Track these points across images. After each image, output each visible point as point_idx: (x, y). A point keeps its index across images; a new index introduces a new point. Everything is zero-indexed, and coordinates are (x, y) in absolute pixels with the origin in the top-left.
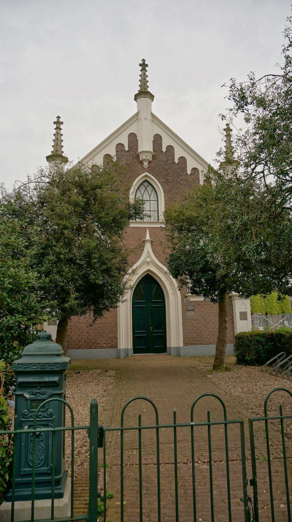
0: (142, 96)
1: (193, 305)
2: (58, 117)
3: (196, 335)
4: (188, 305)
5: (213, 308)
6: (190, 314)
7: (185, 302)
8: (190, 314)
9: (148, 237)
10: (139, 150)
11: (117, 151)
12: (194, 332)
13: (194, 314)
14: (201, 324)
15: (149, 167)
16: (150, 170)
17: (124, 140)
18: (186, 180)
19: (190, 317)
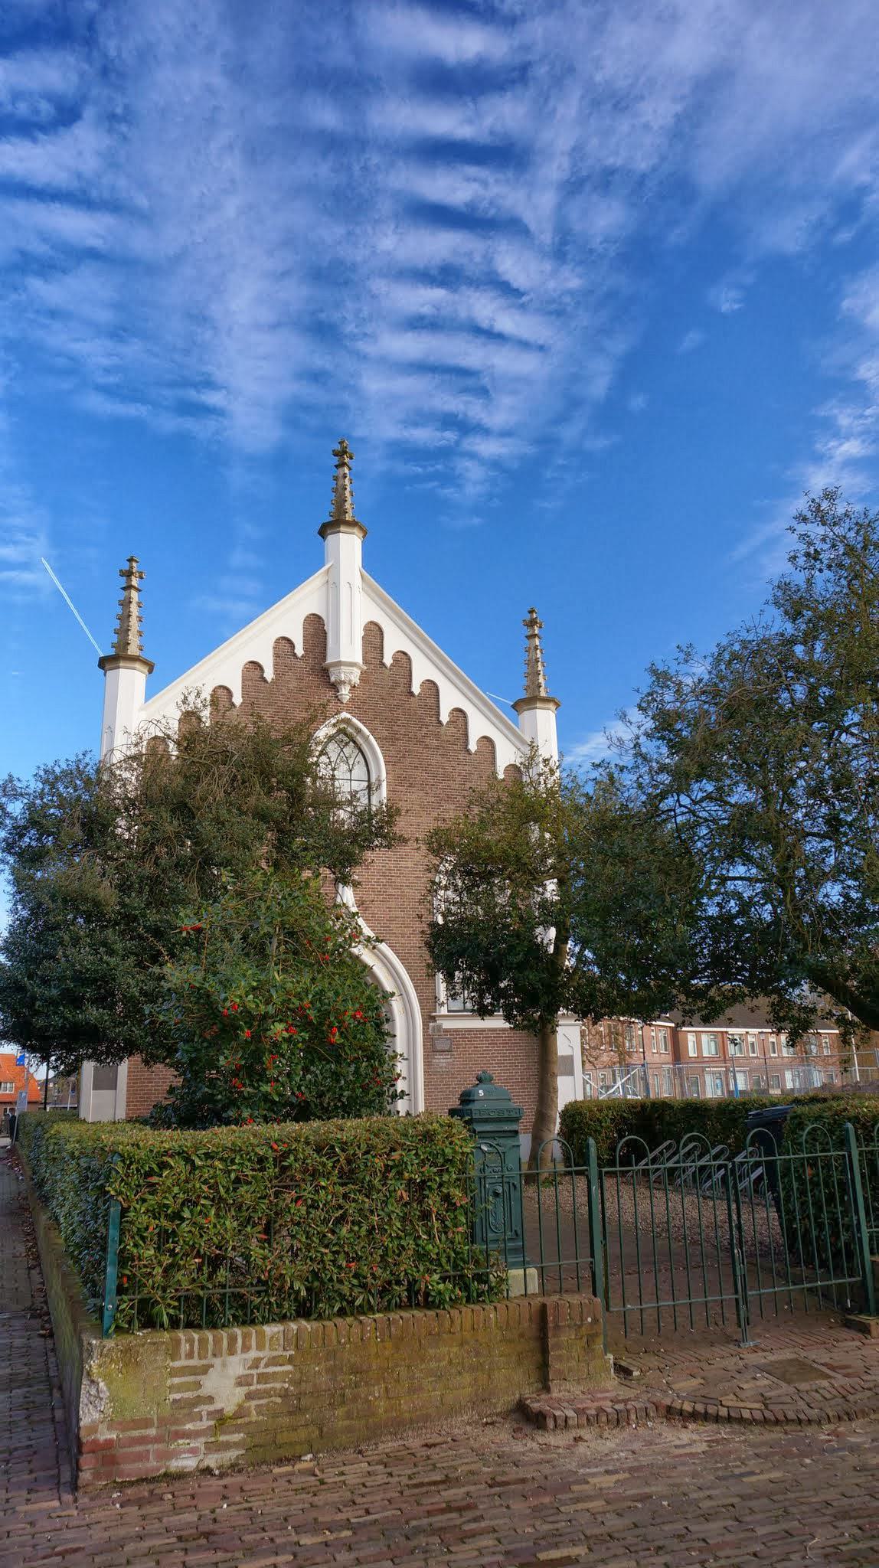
0: (342, 528)
1: (448, 1039)
4: (437, 1039)
7: (430, 1032)
8: (441, 1060)
10: (330, 660)
11: (277, 656)
15: (352, 700)
16: (355, 707)
18: (437, 736)
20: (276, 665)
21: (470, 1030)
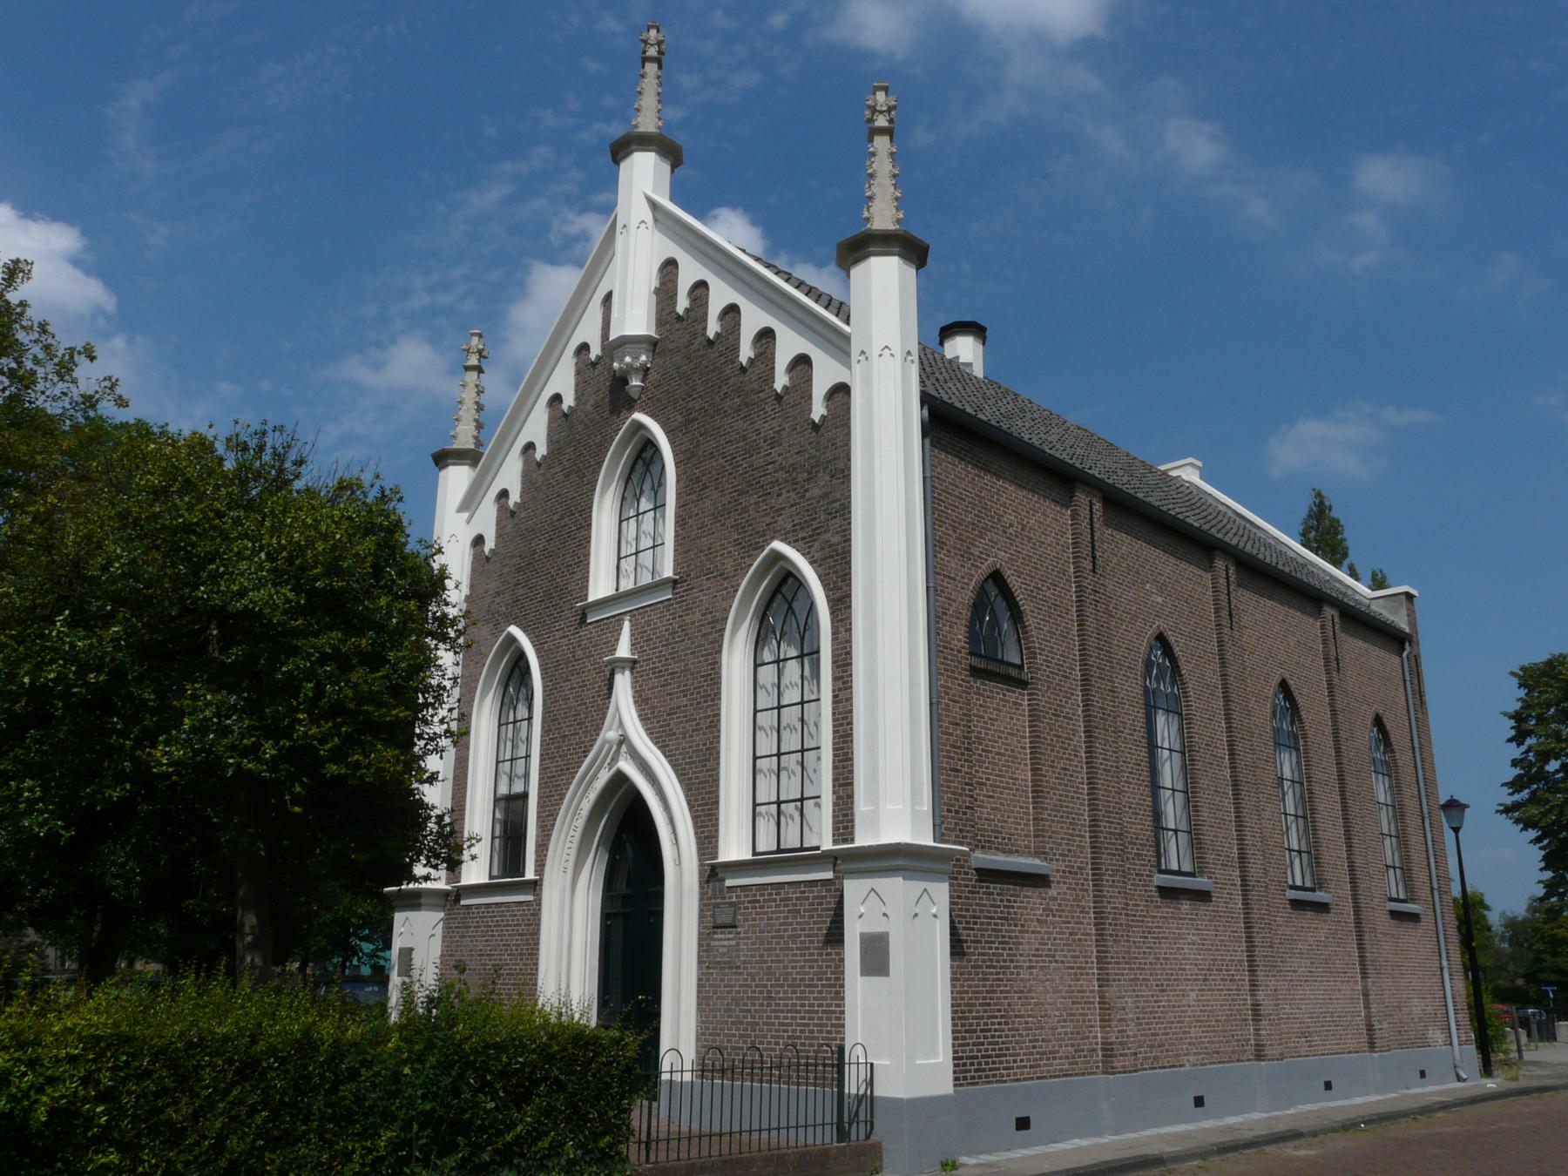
1: (732, 904)
3: (741, 1036)
5: (795, 918)
6: (722, 943)
8: (723, 940)
9: (624, 650)
12: (732, 1023)
13: (734, 943)
14: (757, 986)
19: (723, 954)
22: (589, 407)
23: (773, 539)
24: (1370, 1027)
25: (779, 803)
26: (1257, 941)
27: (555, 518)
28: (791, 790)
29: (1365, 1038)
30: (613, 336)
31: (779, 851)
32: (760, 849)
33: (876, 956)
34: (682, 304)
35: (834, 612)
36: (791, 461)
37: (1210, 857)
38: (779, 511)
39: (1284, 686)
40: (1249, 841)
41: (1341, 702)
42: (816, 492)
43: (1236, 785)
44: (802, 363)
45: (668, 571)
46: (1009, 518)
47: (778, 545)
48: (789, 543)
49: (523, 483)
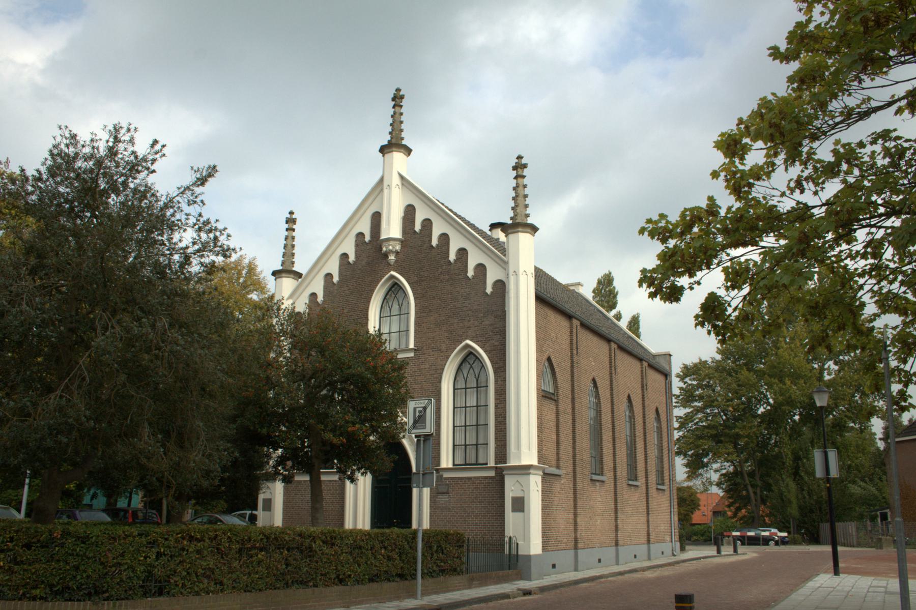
1: (446, 485)
2: (291, 213)
8: (443, 499)
10: (383, 237)
11: (357, 246)
15: (396, 261)
17: (364, 227)
20: (356, 252)
21: (461, 478)
22: (364, 263)
23: (466, 339)
24: (648, 535)
25: (466, 445)
26: (619, 500)
27: (345, 311)
28: (471, 440)
29: (646, 539)
30: (383, 237)
31: (466, 464)
32: (456, 463)
33: (520, 505)
34: (418, 228)
35: (496, 371)
36: (475, 307)
37: (605, 467)
38: (469, 328)
39: (629, 397)
40: (618, 461)
41: (646, 403)
42: (487, 323)
43: (614, 439)
44: (481, 269)
45: (412, 346)
46: (553, 334)
47: (468, 342)
48: (474, 342)
49: (324, 291)
